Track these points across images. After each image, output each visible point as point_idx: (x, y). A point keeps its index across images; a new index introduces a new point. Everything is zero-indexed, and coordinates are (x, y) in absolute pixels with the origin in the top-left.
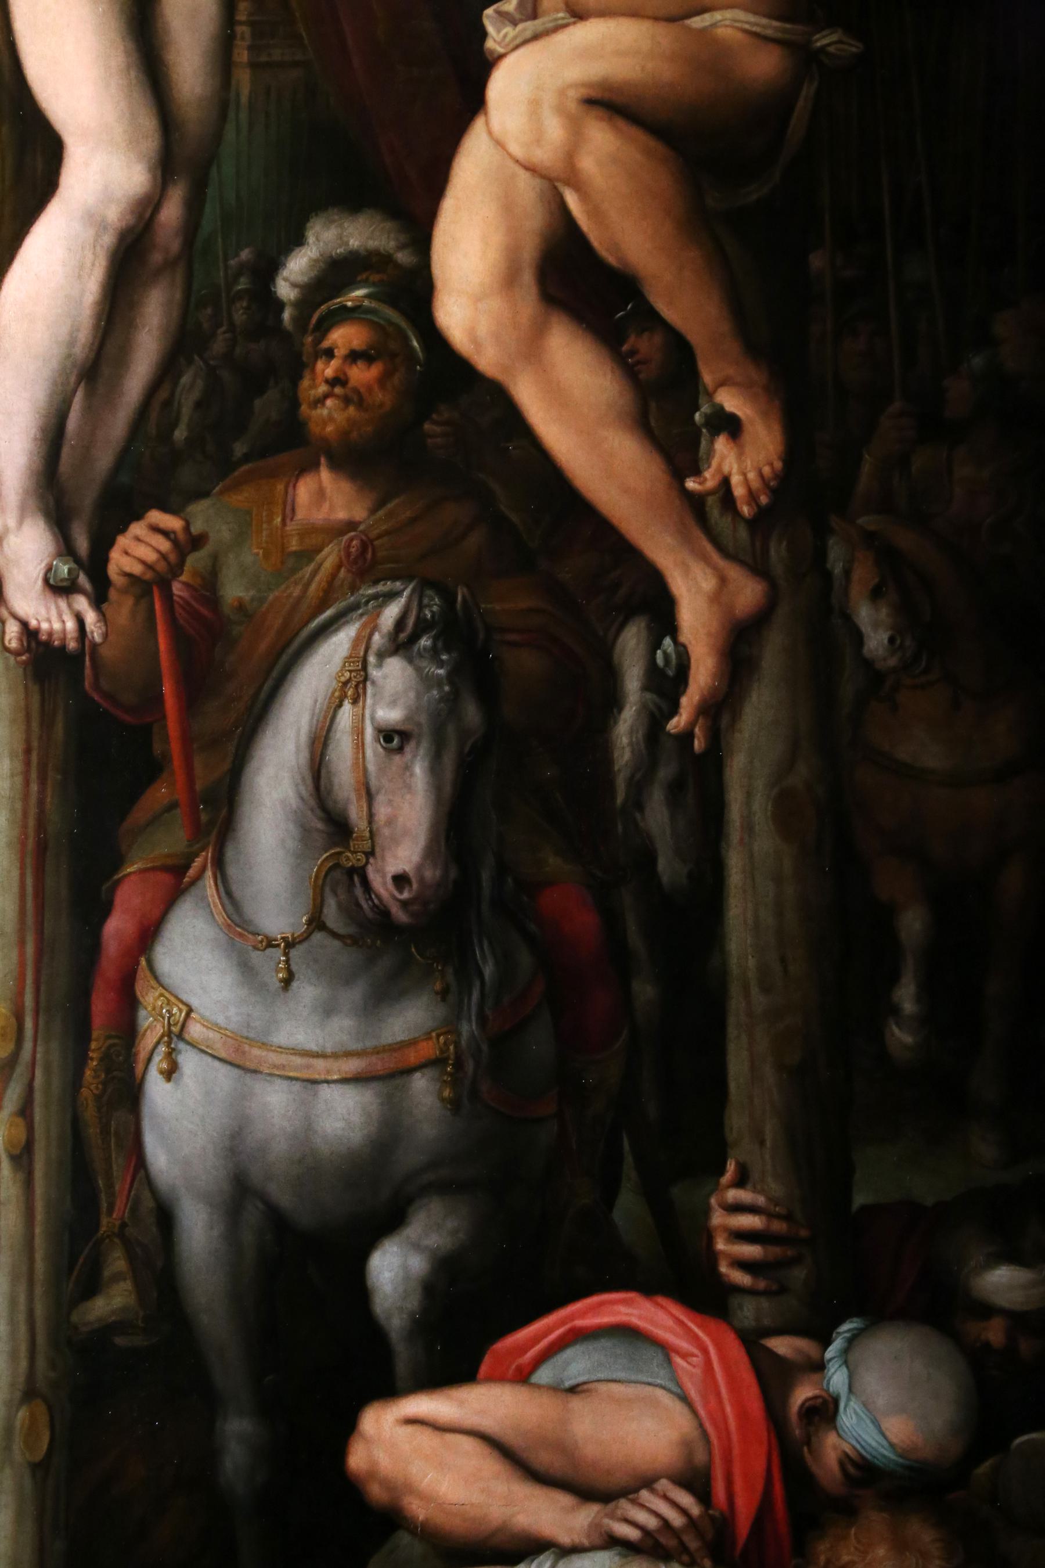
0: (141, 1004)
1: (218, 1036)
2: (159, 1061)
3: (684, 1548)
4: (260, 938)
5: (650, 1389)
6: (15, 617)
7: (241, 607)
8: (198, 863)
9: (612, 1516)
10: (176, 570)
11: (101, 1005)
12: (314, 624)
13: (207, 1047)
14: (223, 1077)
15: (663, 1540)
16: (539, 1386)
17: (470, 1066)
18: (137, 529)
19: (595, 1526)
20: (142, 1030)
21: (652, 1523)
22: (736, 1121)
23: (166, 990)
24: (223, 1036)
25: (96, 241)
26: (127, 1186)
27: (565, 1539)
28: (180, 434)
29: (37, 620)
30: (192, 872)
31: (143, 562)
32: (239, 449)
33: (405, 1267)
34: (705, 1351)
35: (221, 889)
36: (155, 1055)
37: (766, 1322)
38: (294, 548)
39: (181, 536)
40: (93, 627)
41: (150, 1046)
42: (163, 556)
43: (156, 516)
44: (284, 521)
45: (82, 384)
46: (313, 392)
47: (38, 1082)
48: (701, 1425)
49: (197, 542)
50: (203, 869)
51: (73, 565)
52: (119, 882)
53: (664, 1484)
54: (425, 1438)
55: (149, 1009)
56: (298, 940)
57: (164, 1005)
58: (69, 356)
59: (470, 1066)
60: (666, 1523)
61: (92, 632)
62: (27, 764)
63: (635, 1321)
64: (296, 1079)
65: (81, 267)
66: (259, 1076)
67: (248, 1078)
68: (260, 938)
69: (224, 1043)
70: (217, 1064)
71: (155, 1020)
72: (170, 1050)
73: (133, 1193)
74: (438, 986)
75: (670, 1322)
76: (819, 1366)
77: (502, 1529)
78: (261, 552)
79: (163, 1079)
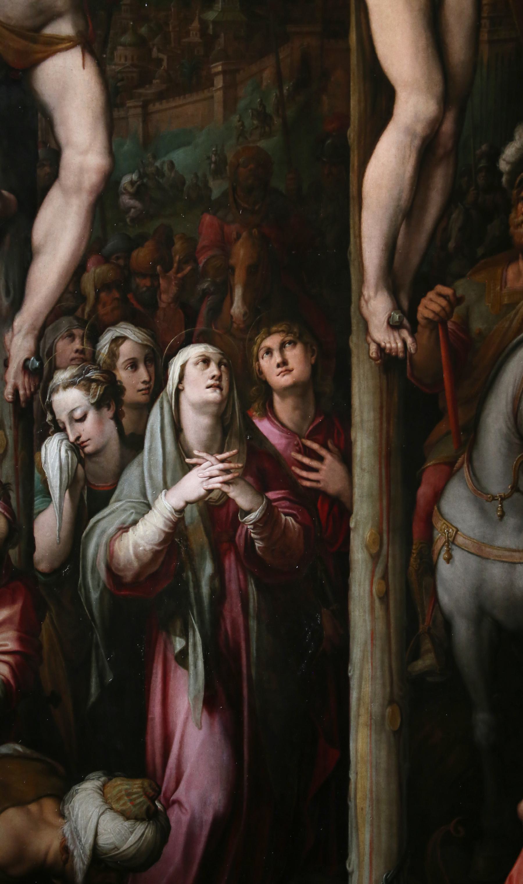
0: (435, 528)
1: (470, 542)
2: (443, 554)
4: (489, 496)
6: (374, 341)
7: (480, 333)
8: (460, 460)
10: (449, 315)
11: (417, 528)
12: (515, 341)
13: (466, 547)
14: (473, 561)
18: (431, 295)
20: (436, 540)
23: (446, 521)
24: (473, 542)
25: (411, 143)
26: (431, 611)
28: (451, 245)
29: (384, 342)
30: (457, 465)
31: (434, 312)
32: (480, 251)
35: (471, 473)
36: (442, 551)
38: (506, 302)
39: (452, 298)
40: (410, 346)
41: (440, 547)
42: (443, 309)
43: (440, 288)
44: (501, 289)
45: (404, 221)
46: (516, 220)
47: (390, 564)
49: (459, 300)
50: (463, 464)
51: (401, 315)
52: (424, 470)
55: (439, 530)
56: (507, 497)
57: (445, 528)
58: (398, 206)
61: (410, 348)
62: (381, 413)
64: (506, 562)
65: (404, 158)
66: (489, 561)
68: (489, 496)
69: (473, 546)
70: (470, 555)
71: (442, 535)
72: (449, 549)
73: (433, 614)
78: (490, 304)
79: (446, 562)
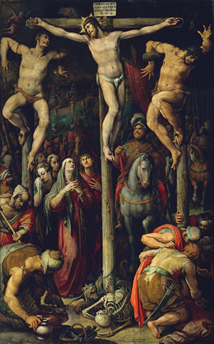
17: (152, 203)
19: (164, 246)
21: (170, 245)
22: (178, 207)
33: (146, 222)
53: (171, 242)
60: (171, 246)
76: (186, 231)
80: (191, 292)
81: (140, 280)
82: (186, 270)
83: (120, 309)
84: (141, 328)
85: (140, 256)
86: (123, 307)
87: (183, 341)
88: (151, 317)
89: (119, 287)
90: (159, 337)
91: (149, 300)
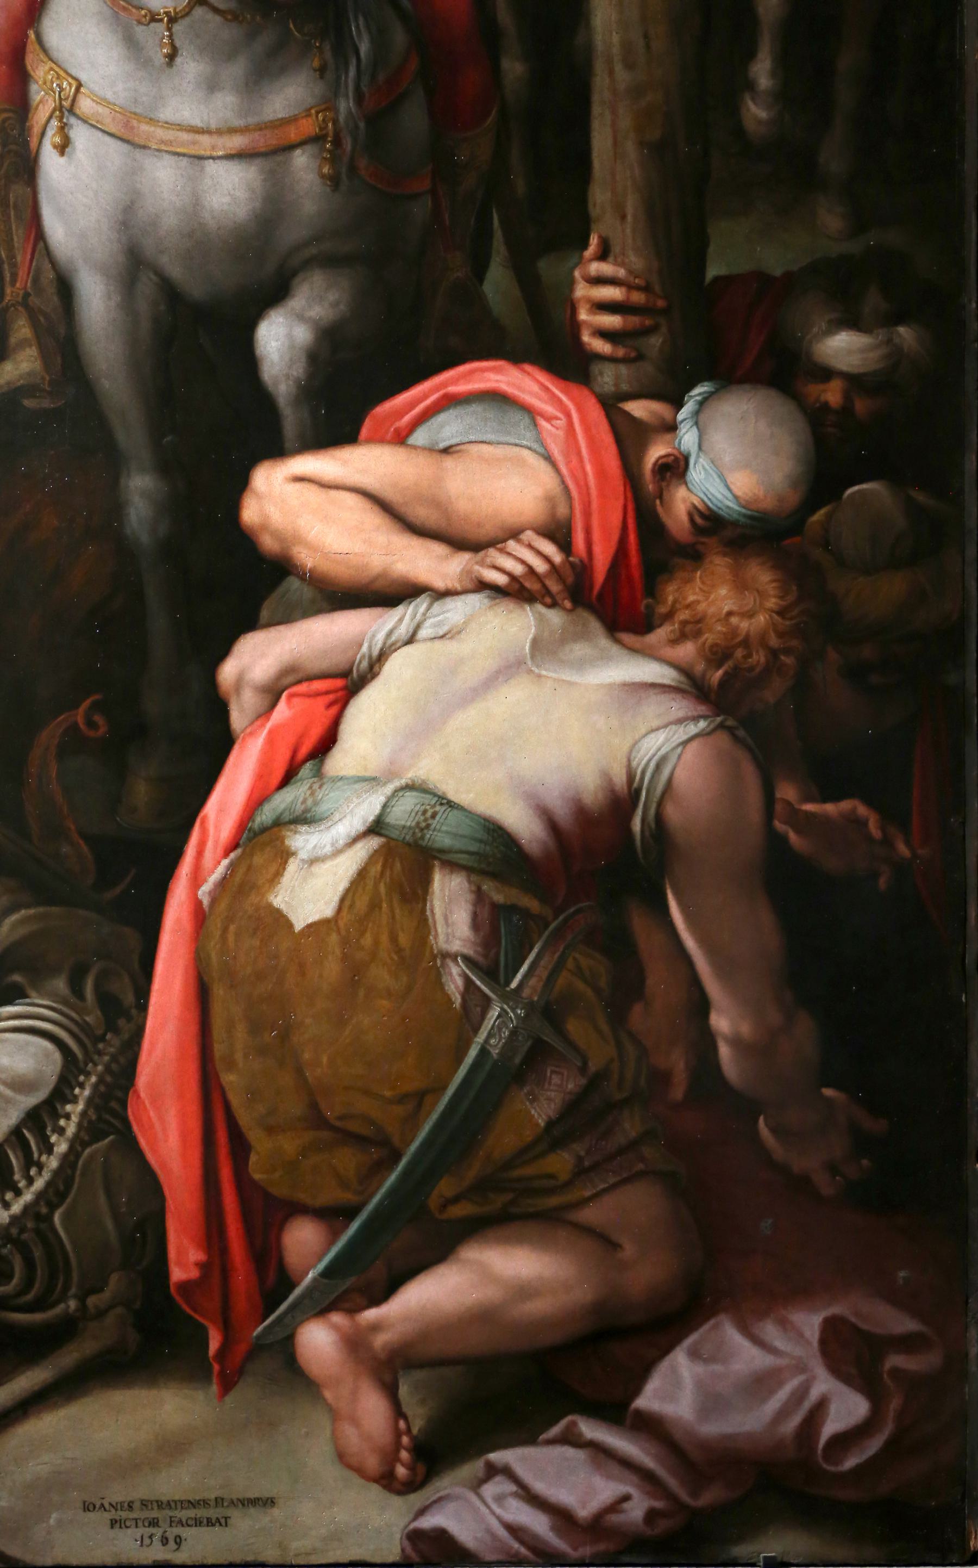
0: (33, 77)
1: (107, 111)
3: (548, 592)
4: (143, 12)
5: (517, 449)
9: (482, 563)
13: (98, 122)
15: (528, 584)
16: (415, 447)
17: (348, 144)
19: (467, 572)
21: (518, 569)
22: (599, 196)
23: (55, 63)
24: (113, 112)
26: (29, 257)
27: (440, 584)
33: (290, 336)
34: (568, 416)
36: (48, 129)
37: (625, 387)
48: (563, 482)
53: (529, 535)
54: (311, 494)
55: (40, 83)
56: (180, 15)
57: (54, 79)
59: (348, 144)
60: (531, 570)
63: (504, 387)
64: (184, 155)
66: (148, 152)
67: (138, 154)
68: (143, 12)
69: (114, 119)
70: (107, 139)
71: (46, 94)
72: (63, 125)
73: (34, 264)
74: (316, 63)
75: (536, 388)
76: (672, 428)
77: (383, 575)
79: (58, 153)
80: (721, 1022)
81: (223, 905)
82: (672, 813)
83: (28, 1197)
84: (227, 1386)
85: (228, 671)
86: (57, 1173)
87: (636, 1510)
88: (328, 1273)
89: (17, 978)
90: (401, 1471)
91: (314, 1106)
